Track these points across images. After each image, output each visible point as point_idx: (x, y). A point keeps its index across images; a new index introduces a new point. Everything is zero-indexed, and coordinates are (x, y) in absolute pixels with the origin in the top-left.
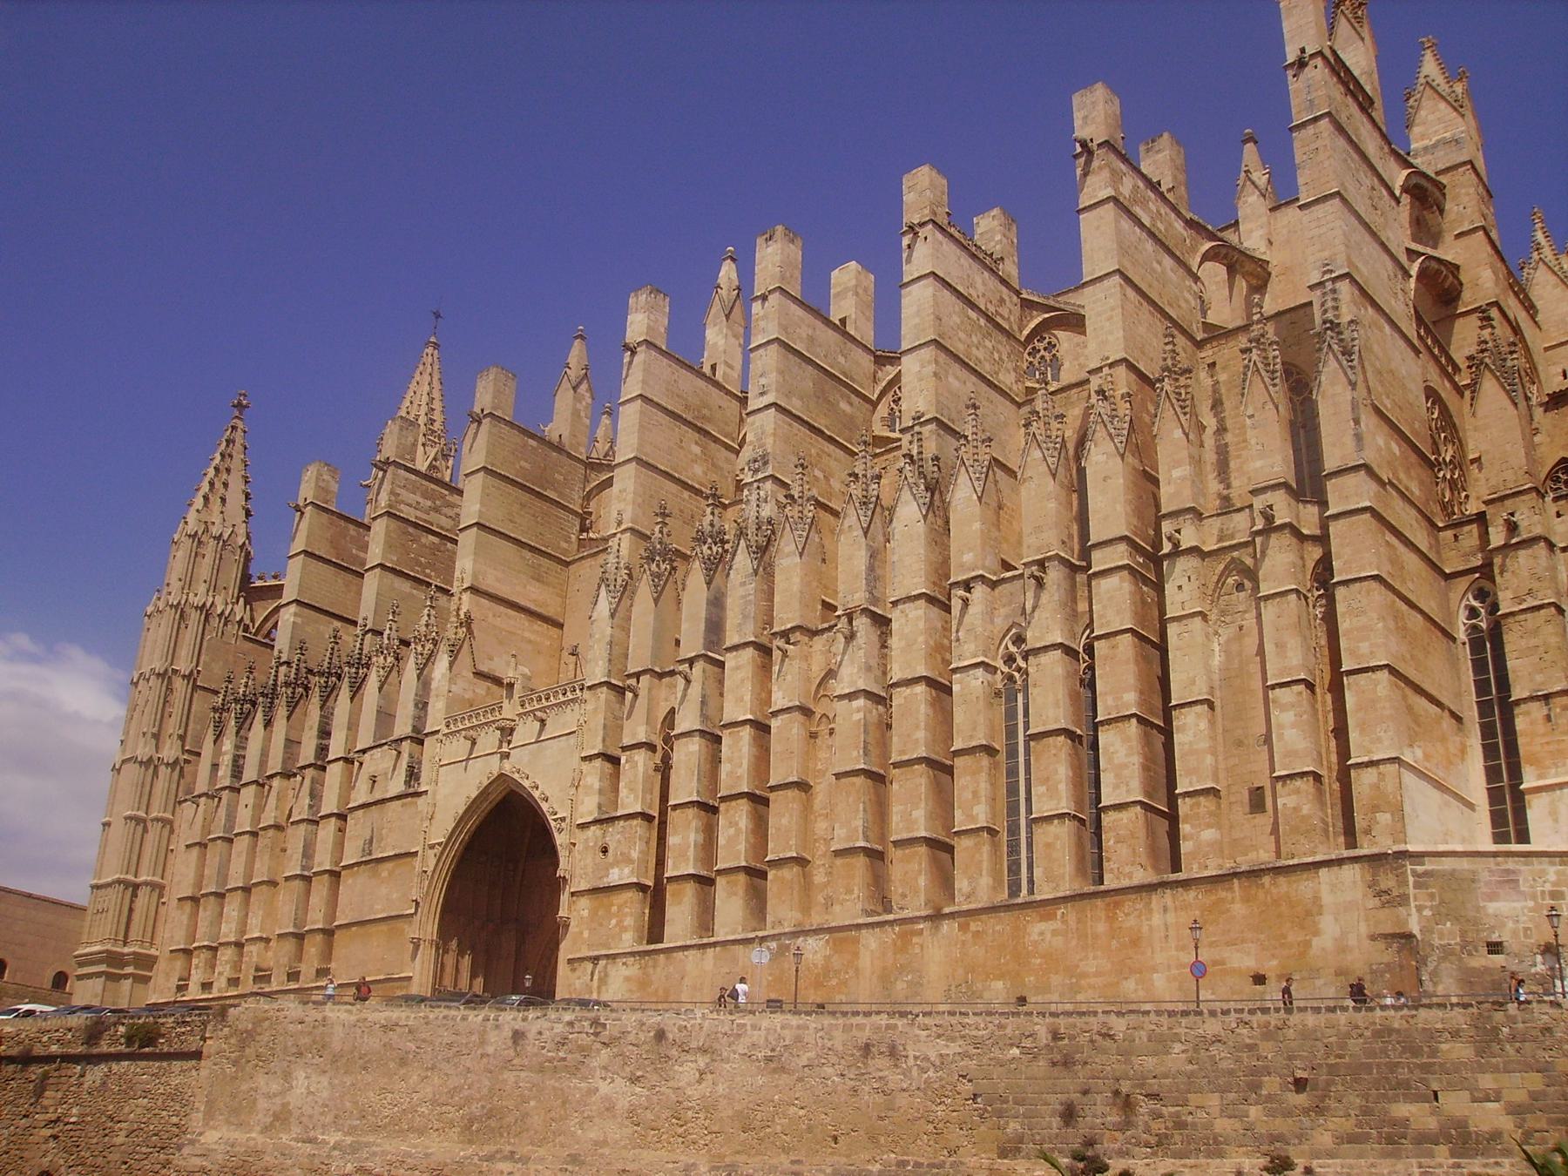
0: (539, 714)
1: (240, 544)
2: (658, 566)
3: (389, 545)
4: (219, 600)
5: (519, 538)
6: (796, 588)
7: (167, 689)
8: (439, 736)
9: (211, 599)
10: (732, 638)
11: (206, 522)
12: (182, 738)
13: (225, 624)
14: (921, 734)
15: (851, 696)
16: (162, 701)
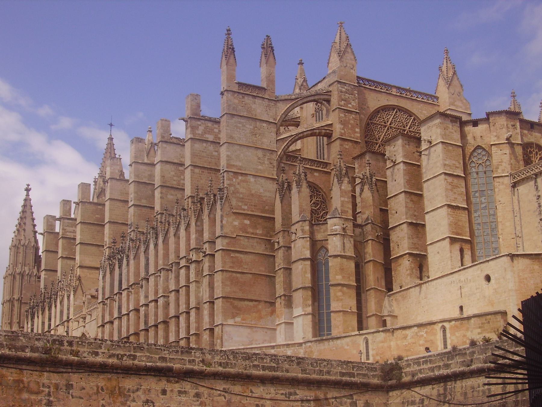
0: (89, 313)
1: (32, 245)
2: (120, 256)
3: (64, 249)
4: (27, 269)
5: (98, 244)
6: (133, 271)
7: (12, 305)
8: (72, 320)
9: (23, 270)
10: (123, 288)
11: (19, 240)
12: (19, 323)
13: (30, 278)
14: (153, 318)
15: (142, 306)
16: (10, 310)
